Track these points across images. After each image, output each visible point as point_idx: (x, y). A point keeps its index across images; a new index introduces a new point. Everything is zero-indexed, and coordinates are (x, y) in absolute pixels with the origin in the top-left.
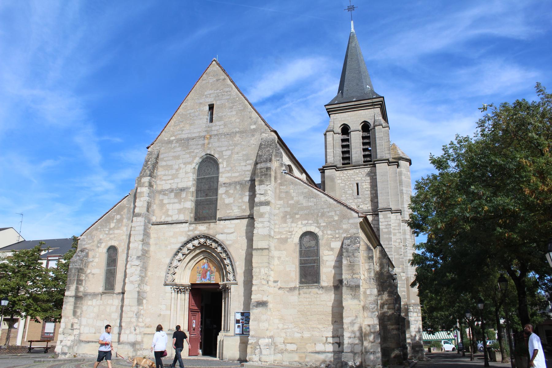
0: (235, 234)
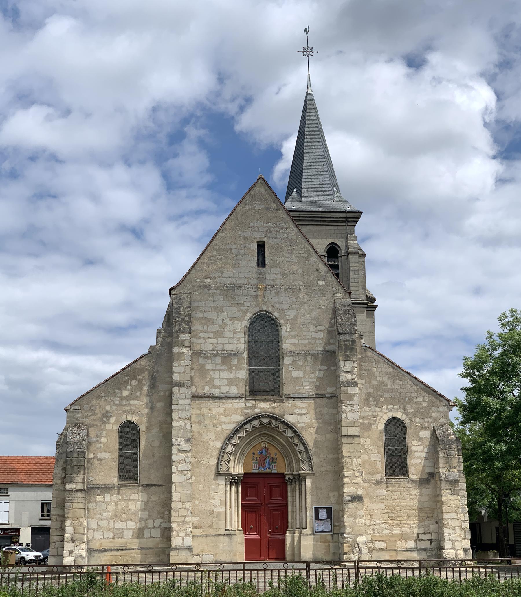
0: (308, 416)
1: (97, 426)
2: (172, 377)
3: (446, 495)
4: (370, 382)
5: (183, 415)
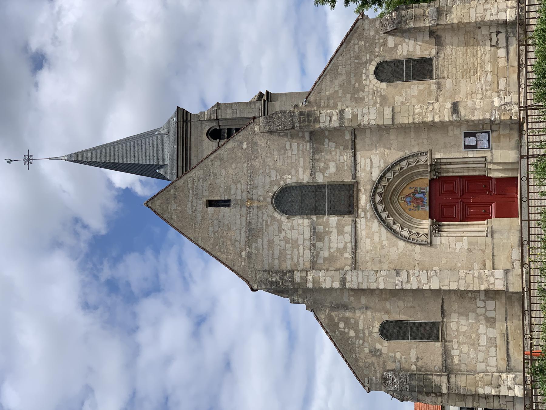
0: (373, 157)
1: (384, 362)
2: (336, 289)
3: (452, 19)
4: (341, 97)
5: (373, 278)
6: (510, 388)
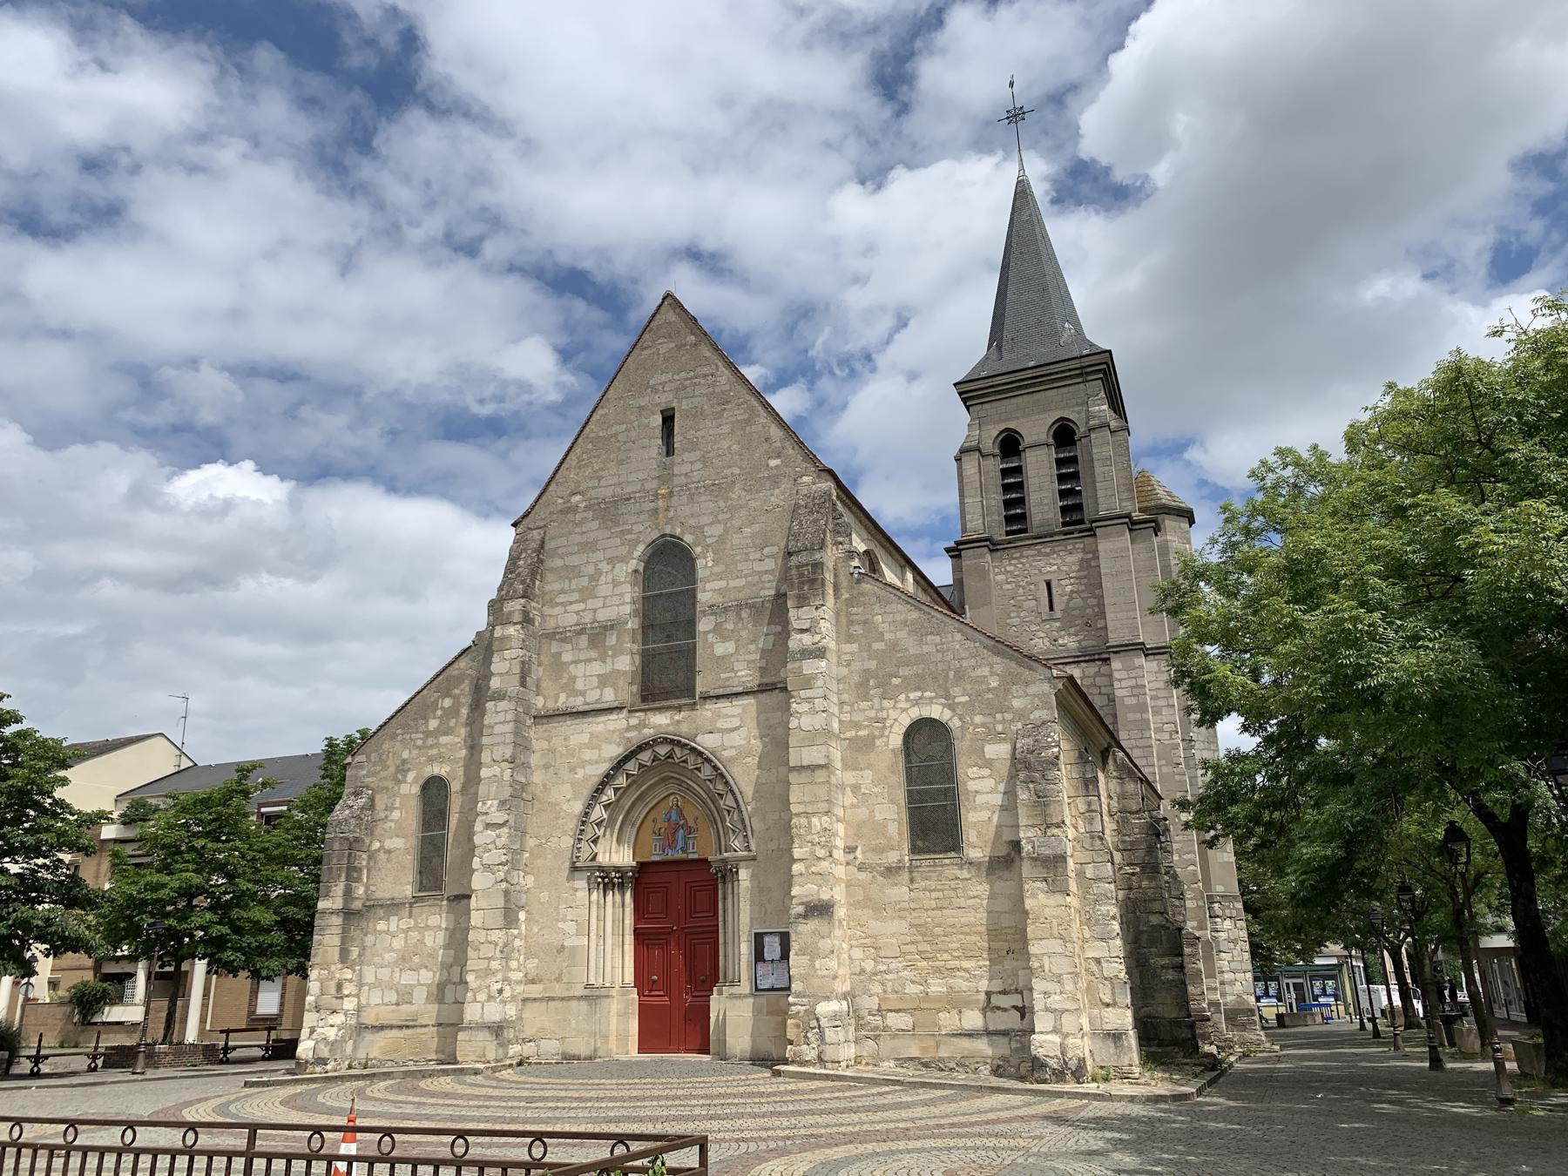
0: (743, 732)
3: (1034, 896)
6: (312, 1030)
